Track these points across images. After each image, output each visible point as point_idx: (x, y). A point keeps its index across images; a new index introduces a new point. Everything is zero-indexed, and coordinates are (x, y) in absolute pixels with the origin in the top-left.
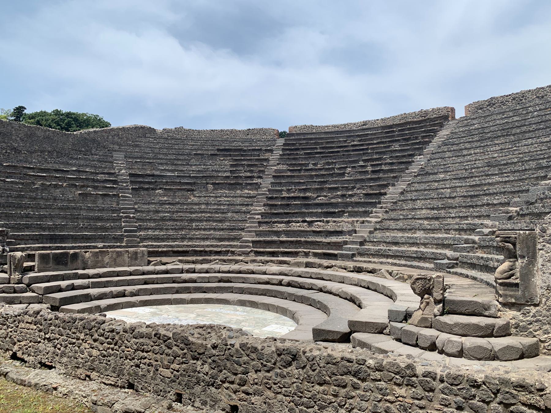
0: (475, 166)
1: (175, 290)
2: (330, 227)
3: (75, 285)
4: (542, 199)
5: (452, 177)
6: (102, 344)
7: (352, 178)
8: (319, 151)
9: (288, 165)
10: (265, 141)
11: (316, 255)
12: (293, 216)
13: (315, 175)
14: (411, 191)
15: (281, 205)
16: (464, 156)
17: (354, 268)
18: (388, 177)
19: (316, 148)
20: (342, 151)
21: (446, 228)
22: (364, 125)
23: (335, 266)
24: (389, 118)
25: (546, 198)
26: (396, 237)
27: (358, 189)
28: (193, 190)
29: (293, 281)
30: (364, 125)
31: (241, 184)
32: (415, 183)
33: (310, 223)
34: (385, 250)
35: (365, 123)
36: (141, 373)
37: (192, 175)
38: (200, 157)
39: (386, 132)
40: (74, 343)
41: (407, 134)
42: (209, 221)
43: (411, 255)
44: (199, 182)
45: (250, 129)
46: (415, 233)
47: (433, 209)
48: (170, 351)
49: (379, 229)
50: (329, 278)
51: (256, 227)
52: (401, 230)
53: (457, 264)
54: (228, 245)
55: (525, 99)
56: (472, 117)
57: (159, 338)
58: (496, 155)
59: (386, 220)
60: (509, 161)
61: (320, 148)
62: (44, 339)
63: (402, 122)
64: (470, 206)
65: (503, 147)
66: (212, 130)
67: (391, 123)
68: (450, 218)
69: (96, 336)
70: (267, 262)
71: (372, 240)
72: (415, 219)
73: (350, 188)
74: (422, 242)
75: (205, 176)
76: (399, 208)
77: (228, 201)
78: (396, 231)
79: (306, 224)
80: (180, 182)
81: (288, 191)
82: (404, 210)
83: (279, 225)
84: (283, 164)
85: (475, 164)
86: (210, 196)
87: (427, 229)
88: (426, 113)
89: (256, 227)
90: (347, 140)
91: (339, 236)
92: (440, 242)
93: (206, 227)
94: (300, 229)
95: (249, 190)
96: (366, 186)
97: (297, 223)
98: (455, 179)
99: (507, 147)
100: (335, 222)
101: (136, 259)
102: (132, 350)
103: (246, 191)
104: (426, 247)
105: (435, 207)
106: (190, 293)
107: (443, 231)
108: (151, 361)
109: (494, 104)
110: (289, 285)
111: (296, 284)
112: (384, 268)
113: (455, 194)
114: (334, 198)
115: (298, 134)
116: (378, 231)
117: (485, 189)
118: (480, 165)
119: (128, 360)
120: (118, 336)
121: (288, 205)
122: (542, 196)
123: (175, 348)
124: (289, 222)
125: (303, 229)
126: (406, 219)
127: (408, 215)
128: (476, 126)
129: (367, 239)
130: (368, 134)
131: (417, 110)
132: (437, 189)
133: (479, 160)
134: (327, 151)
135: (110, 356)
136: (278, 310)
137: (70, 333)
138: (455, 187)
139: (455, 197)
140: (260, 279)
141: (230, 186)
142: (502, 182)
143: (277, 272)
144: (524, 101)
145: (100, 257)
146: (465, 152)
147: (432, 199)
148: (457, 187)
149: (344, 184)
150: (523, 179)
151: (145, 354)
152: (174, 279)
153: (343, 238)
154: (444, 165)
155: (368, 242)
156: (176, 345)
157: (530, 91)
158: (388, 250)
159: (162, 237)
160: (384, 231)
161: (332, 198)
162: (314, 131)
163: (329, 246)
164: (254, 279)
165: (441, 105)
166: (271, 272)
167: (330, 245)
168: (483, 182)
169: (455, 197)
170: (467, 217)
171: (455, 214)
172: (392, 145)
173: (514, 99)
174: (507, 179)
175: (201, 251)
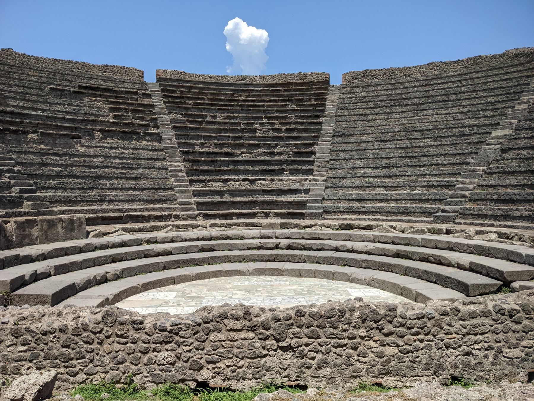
1: (162, 265)
2: (275, 186)
4: (498, 161)
5: (374, 139)
6: (402, 337)
7: (264, 135)
8: (206, 102)
9: (182, 114)
10: (130, 82)
11: (277, 215)
12: (226, 174)
13: (224, 129)
14: (337, 151)
15: (205, 161)
16: (369, 121)
17: (340, 226)
18: (308, 136)
19: (203, 99)
21: (412, 185)
23: (316, 225)
24: (268, 76)
25: (503, 160)
26: (362, 194)
27: (281, 147)
28: (80, 138)
29: (295, 243)
30: (242, 80)
31: (138, 134)
32: (335, 143)
33: (252, 182)
34: (358, 207)
35: (243, 78)
36: (473, 362)
37: (67, 117)
39: (272, 90)
40: (345, 345)
41: (296, 94)
42: (121, 178)
43: (390, 210)
44: (82, 127)
45: (107, 66)
46: (373, 190)
47: (375, 168)
48: (519, 327)
49: (331, 187)
50: (328, 238)
51: (186, 186)
53: (457, 216)
54: (166, 208)
55: (395, 75)
56: (352, 85)
57: (503, 314)
58: (406, 122)
59: (331, 178)
60: (425, 128)
61: (208, 99)
62: (275, 350)
63: (281, 82)
64: (416, 166)
65: (406, 116)
66: (56, 60)
67: (270, 82)
68: (404, 176)
69: (389, 328)
70: (231, 225)
71: (331, 198)
72: (364, 177)
73: (273, 145)
75: (86, 120)
76: (338, 166)
77: (133, 154)
78: (351, 189)
79: (247, 182)
80: (57, 126)
81: (202, 145)
82: (344, 168)
83: (215, 184)
84: (175, 113)
85: (392, 128)
86: (102, 147)
87: (389, 187)
88: (305, 76)
89: (186, 186)
90: (234, 94)
91: (292, 194)
92: (417, 197)
93: (124, 186)
94: (240, 188)
95: (148, 141)
96: (291, 144)
97: (237, 181)
98: (376, 141)
99: (409, 116)
100: (280, 180)
101: (72, 230)
102: (459, 337)
103: (145, 143)
104: (397, 203)
105: (379, 166)
106: (179, 267)
107: (408, 187)
108: (489, 344)
109: (368, 76)
110: (289, 247)
111: (300, 246)
112: (385, 224)
113: (392, 155)
114: (261, 156)
115: (171, 80)
116: (329, 190)
117: (425, 150)
118: (397, 130)
119: (451, 350)
120: (432, 322)
121: (213, 161)
122: (499, 158)
123: (526, 322)
124: (227, 181)
126: (353, 177)
128: (362, 94)
129: (326, 198)
130: (253, 90)
131: (296, 72)
132: (365, 150)
133: (390, 125)
134: (220, 103)
135: (417, 351)
137: (336, 332)
138: (384, 149)
139: (392, 158)
141: (123, 135)
142: (434, 145)
143: (258, 236)
144: (393, 76)
146: (370, 117)
147: (367, 158)
148: (386, 149)
149: (267, 141)
150: (456, 144)
151: (481, 337)
152: (146, 253)
153: (298, 197)
154: (354, 128)
155: (327, 200)
156: (527, 318)
157: (398, 69)
158: (361, 206)
159: (75, 199)
160: (337, 189)
161: (258, 155)
162: (187, 79)
163: (289, 206)
164: (243, 245)
166: (251, 236)
167: (291, 204)
168: (414, 145)
169: (392, 158)
170: (425, 175)
171: (411, 173)
172: (289, 105)
173: (385, 74)
174: (439, 143)
175: (138, 217)
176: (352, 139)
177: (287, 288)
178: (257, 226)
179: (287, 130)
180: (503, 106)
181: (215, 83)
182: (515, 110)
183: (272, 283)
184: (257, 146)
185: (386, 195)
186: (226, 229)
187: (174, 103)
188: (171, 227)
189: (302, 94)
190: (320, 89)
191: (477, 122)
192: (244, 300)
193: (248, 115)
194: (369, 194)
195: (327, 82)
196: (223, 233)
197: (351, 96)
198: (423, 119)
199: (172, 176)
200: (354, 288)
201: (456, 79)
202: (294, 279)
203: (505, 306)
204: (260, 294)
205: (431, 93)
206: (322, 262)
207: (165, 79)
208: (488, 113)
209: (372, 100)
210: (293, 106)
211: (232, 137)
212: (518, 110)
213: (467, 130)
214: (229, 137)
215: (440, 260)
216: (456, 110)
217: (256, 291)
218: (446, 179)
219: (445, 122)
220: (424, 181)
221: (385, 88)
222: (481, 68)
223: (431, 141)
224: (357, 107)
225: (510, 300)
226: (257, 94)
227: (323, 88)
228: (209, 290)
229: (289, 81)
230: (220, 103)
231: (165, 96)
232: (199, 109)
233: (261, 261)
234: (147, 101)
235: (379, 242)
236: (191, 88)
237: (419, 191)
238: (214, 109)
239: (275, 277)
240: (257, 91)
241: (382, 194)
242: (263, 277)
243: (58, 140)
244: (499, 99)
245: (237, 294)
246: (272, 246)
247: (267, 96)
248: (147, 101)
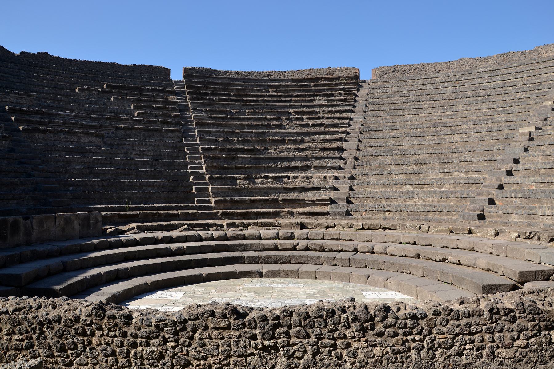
0: (421, 126)
15: (225, 158)
22: (268, 75)
31: (160, 131)
38: (87, 93)
50: (350, 238)
52: (384, 185)
56: (382, 81)
63: (309, 77)
70: (249, 224)
74: (420, 196)
75: (110, 119)
88: (334, 71)
111: (318, 248)
118: (426, 126)
125: (264, 186)
127: (383, 171)
128: (392, 89)
131: (325, 67)
134: (245, 99)
136: (333, 276)
140: (267, 244)
145: (45, 226)
146: (400, 113)
157: (429, 64)
159: (94, 197)
164: (259, 245)
165: (350, 66)
166: (268, 237)
174: (468, 140)
176: (381, 134)
177: (299, 290)
178: (276, 226)
179: (314, 125)
180: (531, 102)
181: (241, 79)
182: (543, 107)
183: (285, 285)
184: (283, 142)
185: (413, 193)
186: (243, 229)
187: (199, 99)
188: (186, 226)
189: (331, 89)
191: (505, 118)
192: (251, 302)
193: (273, 110)
194: (396, 192)
195: (357, 77)
196: (239, 232)
197: (381, 90)
198: (453, 115)
199: (192, 173)
200: (370, 290)
201: (486, 75)
202: (309, 281)
203: (498, 306)
204: (270, 296)
205: (461, 89)
206: (340, 264)
207: (192, 76)
208: (515, 109)
209: (402, 95)
210: (321, 100)
211: (255, 133)
212: (546, 106)
213: (495, 127)
214: (252, 132)
215: (459, 261)
216: (485, 105)
217: (266, 293)
218: (474, 176)
219: (475, 118)
220: (452, 179)
221: (415, 83)
222: (511, 64)
223: (460, 137)
224: (387, 102)
225: (504, 300)
226: (284, 89)
227: (352, 83)
228: (217, 292)
229: (318, 76)
230: (245, 99)
232: (223, 105)
233: (276, 262)
235: (401, 243)
236: (216, 84)
237: (446, 188)
238: (238, 105)
239: (289, 279)
240: (284, 86)
241: (407, 193)
242: (276, 279)
243: (83, 138)
244: (528, 95)
245: (245, 296)
246: (290, 247)
247: (294, 91)
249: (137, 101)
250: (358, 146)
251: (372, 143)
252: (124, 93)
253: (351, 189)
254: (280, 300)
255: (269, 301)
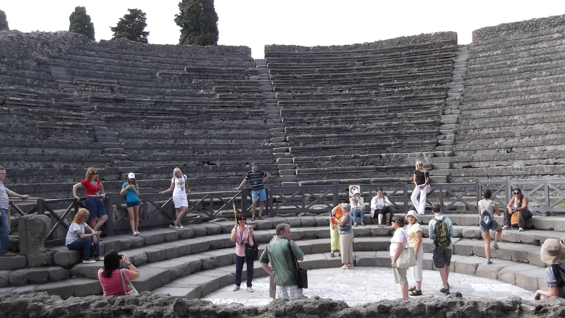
3: (135, 259)
15: (312, 138)
20: (349, 75)
41: (418, 58)
75: (192, 103)
80: (164, 110)
190: (446, 50)
192: (344, 294)
195: (455, 42)
209: (509, 58)
231: (273, 72)
234: (253, 78)
246: (385, 233)
248: (253, 78)
249: (219, 83)
250: (458, 119)
251: (475, 114)
252: (205, 76)
253: (451, 167)
254: (376, 292)
255: (364, 293)
